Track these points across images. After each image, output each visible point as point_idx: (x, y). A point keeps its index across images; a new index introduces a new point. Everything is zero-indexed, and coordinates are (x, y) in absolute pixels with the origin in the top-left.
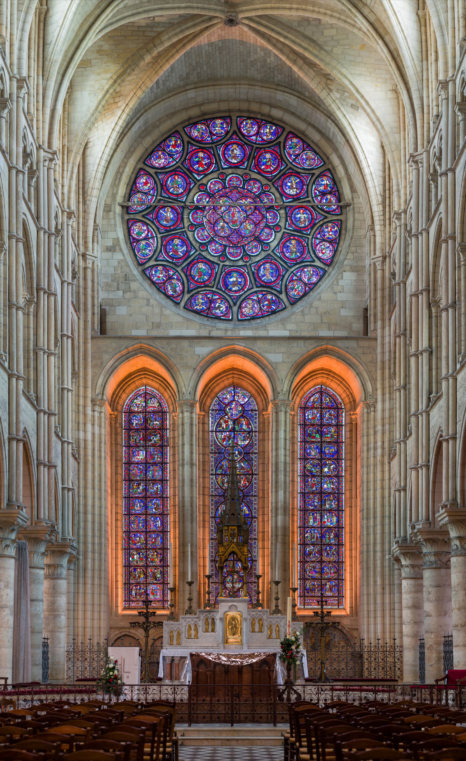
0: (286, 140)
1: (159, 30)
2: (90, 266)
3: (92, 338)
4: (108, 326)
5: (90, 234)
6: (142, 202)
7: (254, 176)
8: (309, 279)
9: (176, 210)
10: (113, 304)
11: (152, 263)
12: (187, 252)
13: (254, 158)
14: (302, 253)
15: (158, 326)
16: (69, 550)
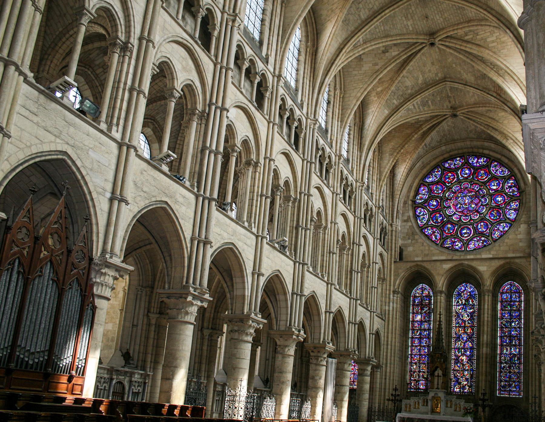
0: (491, 164)
1: (421, 123)
2: (394, 229)
3: (395, 262)
4: (404, 256)
5: (395, 215)
6: (421, 199)
7: (475, 182)
8: (503, 229)
9: (438, 201)
10: (406, 246)
11: (426, 226)
12: (443, 219)
13: (475, 174)
14: (500, 217)
15: (427, 255)
16: (371, 362)
